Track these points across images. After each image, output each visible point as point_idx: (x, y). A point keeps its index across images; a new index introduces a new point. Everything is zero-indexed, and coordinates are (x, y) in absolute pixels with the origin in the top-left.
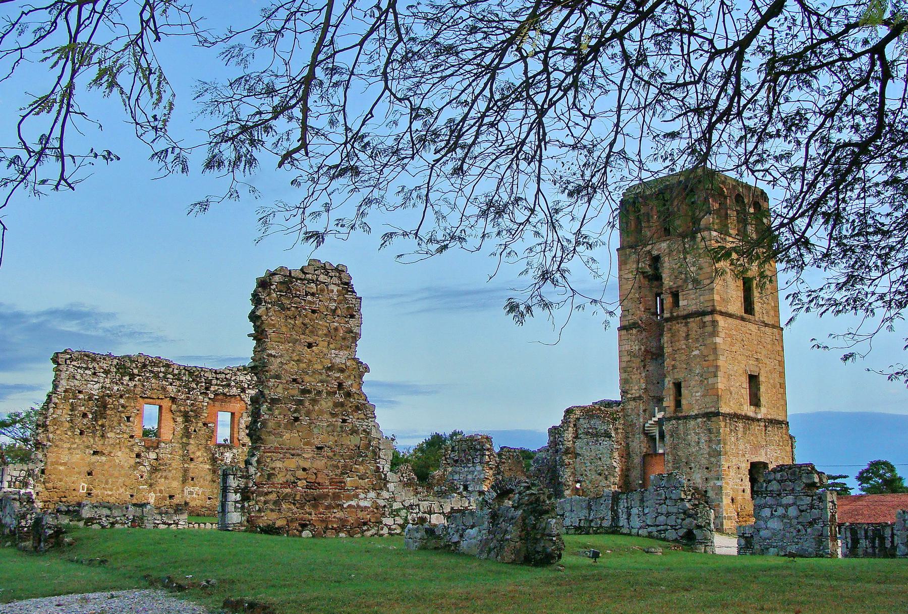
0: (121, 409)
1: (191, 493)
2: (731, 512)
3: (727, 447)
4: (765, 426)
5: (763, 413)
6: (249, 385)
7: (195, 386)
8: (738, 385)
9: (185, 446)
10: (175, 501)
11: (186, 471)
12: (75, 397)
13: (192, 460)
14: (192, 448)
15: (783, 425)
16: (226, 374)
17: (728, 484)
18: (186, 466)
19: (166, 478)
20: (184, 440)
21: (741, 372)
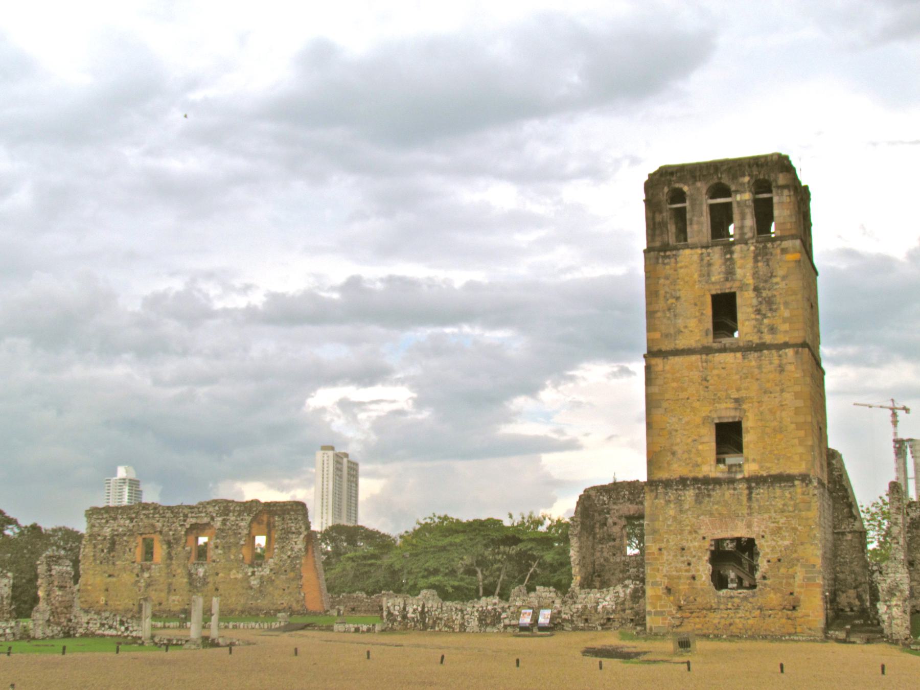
0: (125, 543)
1: (174, 601)
2: (661, 606)
3: (658, 525)
4: (750, 488)
5: (751, 469)
6: (217, 514)
7: (175, 520)
8: (690, 440)
9: (168, 566)
10: (162, 607)
11: (170, 584)
12: (96, 539)
13: (174, 576)
14: (174, 567)
15: (797, 483)
16: (199, 508)
17: (658, 570)
18: (170, 580)
19: (156, 590)
20: (168, 562)
21: (698, 420)
